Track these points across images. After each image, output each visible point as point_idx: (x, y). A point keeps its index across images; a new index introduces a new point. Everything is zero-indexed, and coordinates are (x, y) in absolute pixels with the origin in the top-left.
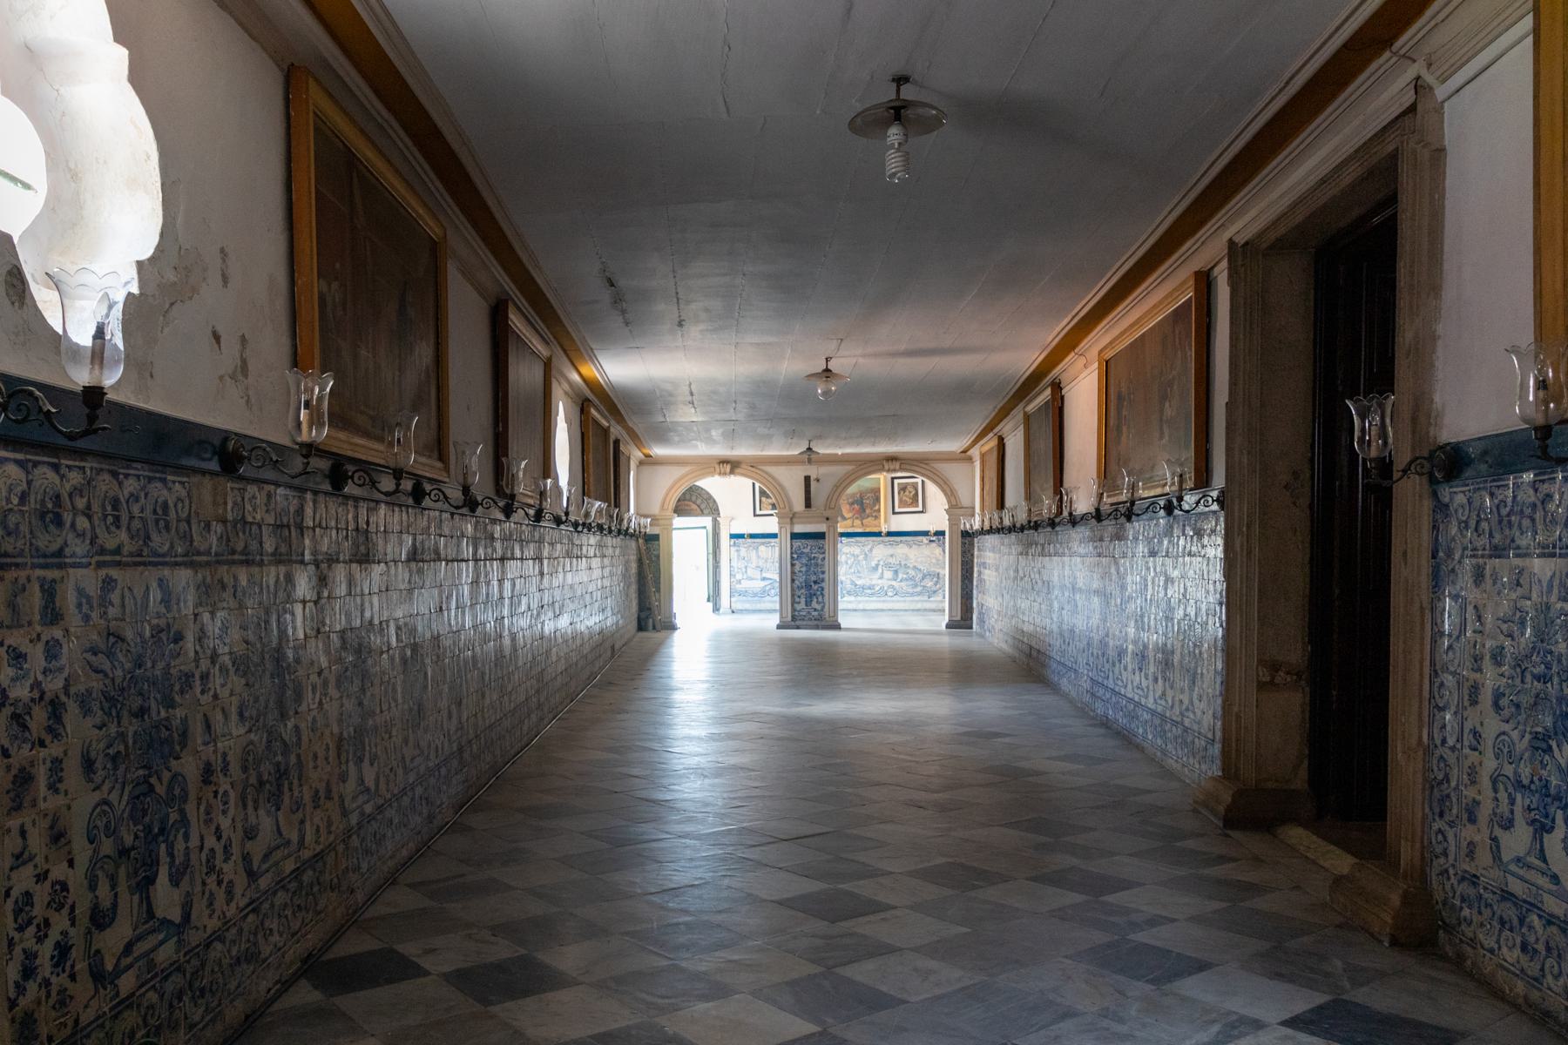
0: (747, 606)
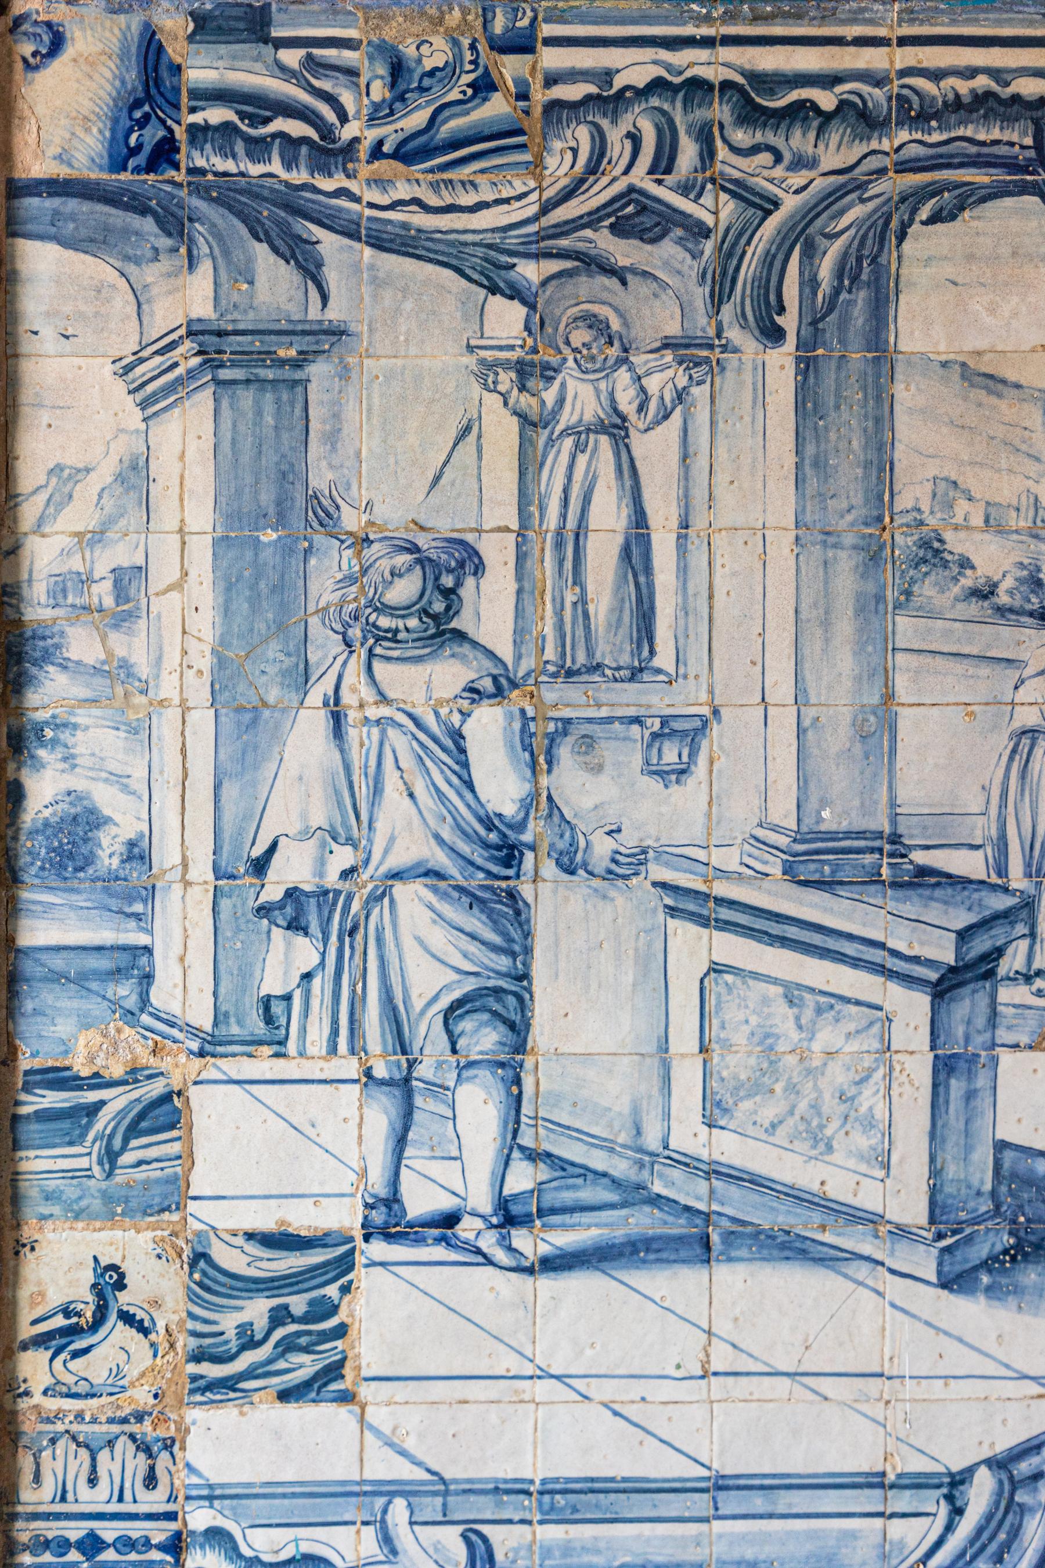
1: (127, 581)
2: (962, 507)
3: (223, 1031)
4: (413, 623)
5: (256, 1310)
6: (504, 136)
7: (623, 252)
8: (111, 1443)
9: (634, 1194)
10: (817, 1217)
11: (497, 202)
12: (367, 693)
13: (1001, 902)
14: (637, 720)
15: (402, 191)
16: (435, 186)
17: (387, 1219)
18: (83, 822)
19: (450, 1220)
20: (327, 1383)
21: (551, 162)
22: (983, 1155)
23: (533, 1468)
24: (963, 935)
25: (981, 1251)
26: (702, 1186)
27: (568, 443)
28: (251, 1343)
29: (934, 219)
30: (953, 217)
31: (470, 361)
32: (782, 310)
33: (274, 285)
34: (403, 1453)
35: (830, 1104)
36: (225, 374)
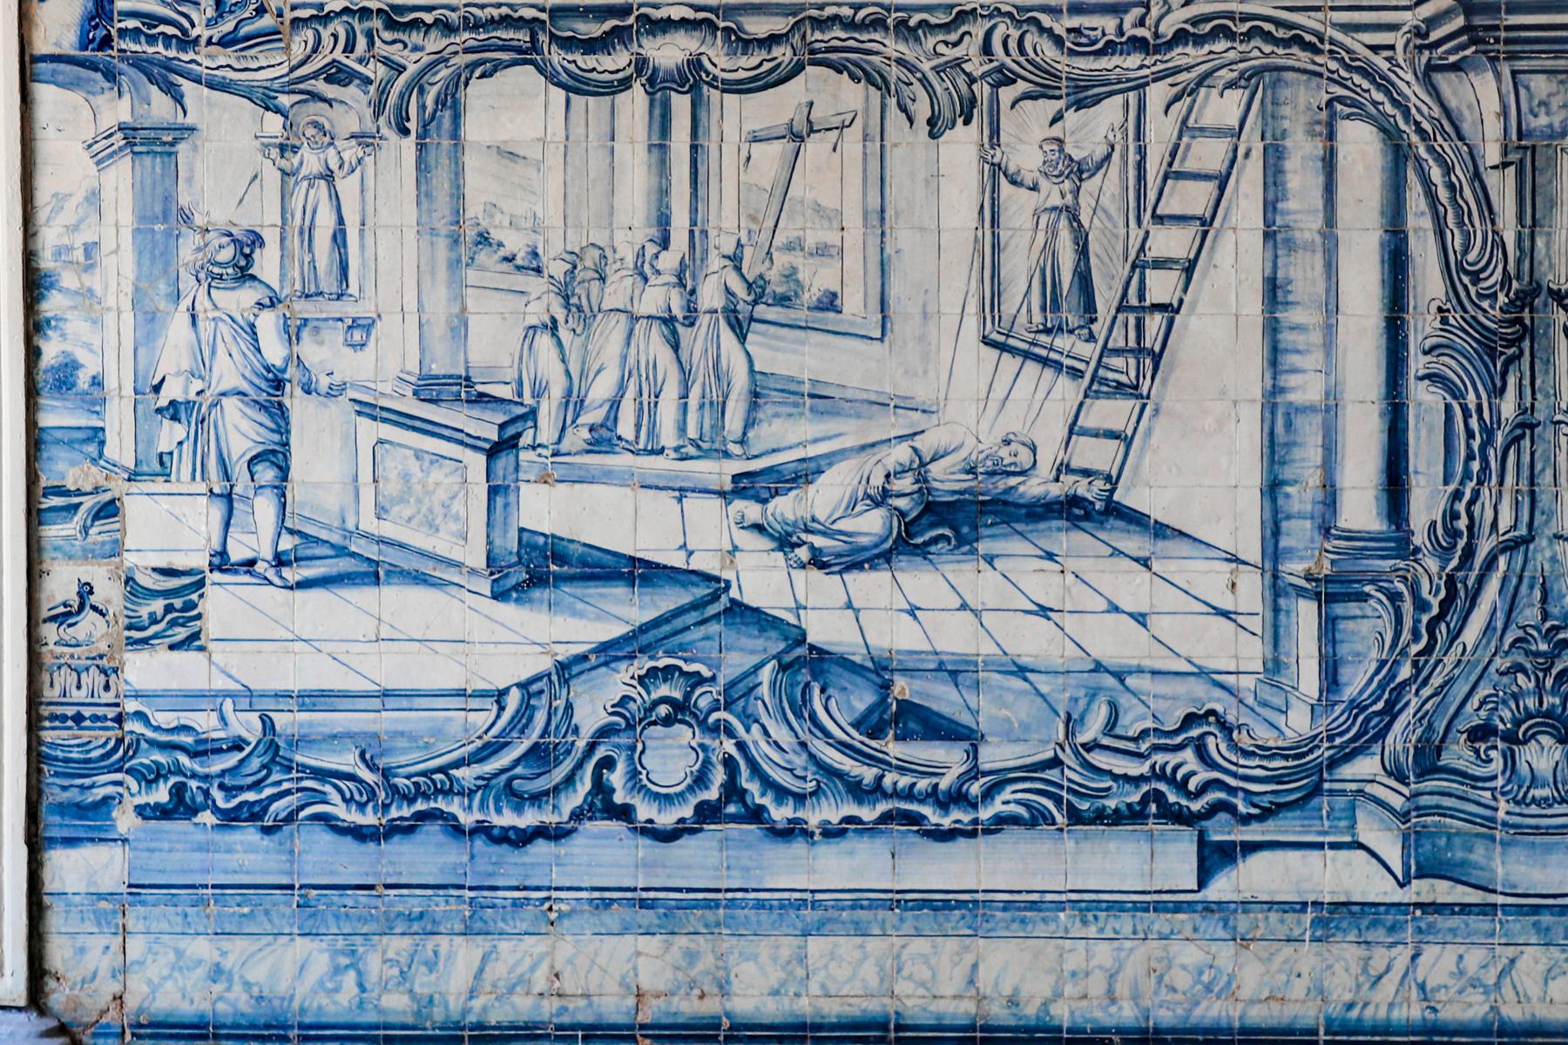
1: (89, 249)
2: (498, 217)
3: (139, 469)
4: (230, 271)
5: (158, 606)
6: (271, 34)
7: (330, 91)
8: (87, 669)
9: (341, 551)
10: (431, 564)
11: (269, 65)
12: (208, 305)
13: (520, 411)
14: (340, 320)
15: (222, 61)
16: (238, 59)
17: (221, 562)
18: (69, 367)
19: (251, 563)
20: (191, 641)
21: (294, 47)
22: (514, 534)
23: (295, 685)
24: (502, 427)
25: (512, 581)
26: (376, 548)
27: (305, 184)
28: (154, 620)
29: (481, 77)
30: (491, 75)
31: (257, 143)
32: (408, 120)
33: (160, 107)
34: (230, 676)
35: (438, 509)
36: (137, 149)
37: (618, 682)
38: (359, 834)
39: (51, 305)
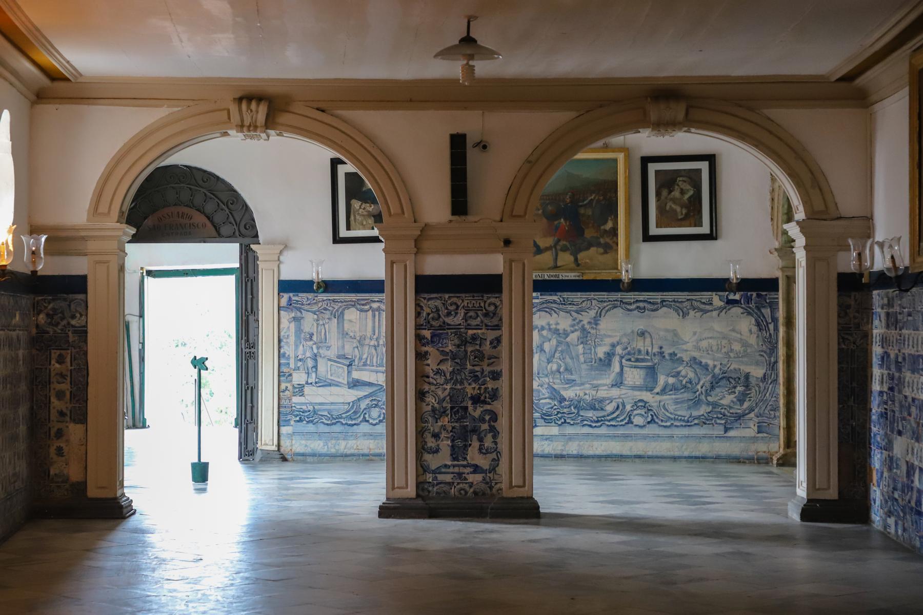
0: (318, 446)
11: (315, 308)
17: (307, 383)
33: (299, 314)
37: (367, 401)
38: (327, 424)
39: (282, 344)
